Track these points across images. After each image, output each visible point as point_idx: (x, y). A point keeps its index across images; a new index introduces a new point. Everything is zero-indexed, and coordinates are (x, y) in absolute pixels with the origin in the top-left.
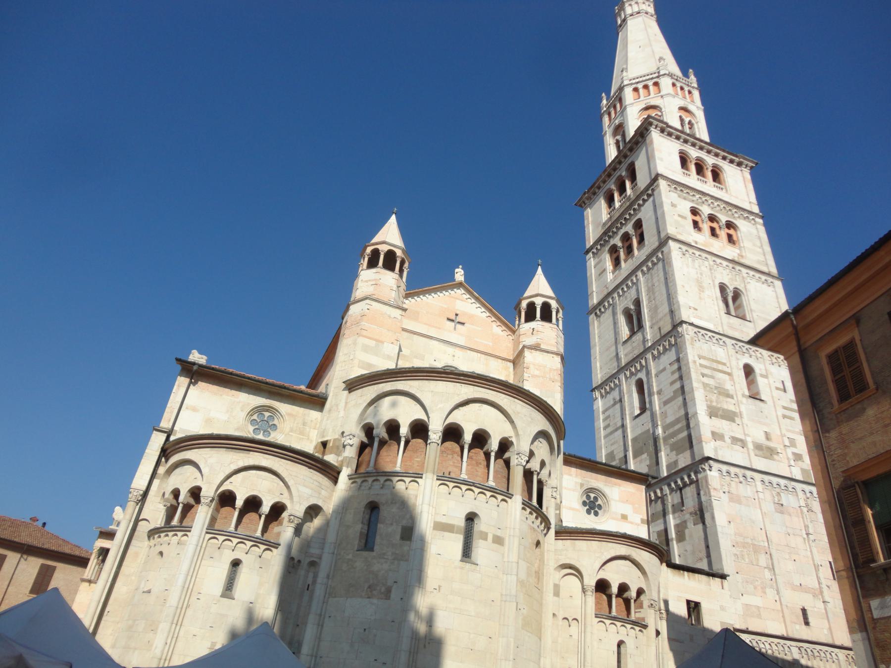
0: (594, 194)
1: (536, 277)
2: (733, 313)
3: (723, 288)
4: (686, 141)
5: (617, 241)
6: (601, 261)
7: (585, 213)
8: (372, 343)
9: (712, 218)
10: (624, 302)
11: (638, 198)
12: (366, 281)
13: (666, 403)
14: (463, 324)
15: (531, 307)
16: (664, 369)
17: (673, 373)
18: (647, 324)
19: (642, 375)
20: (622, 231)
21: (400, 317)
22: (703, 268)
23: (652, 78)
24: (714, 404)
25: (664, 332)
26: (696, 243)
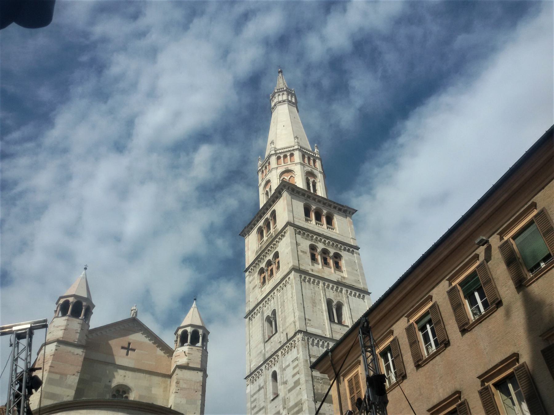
0: (252, 228)
1: (192, 309)
2: (336, 321)
3: (329, 303)
4: (309, 197)
5: (263, 265)
6: (254, 279)
7: (246, 241)
8: (57, 377)
9: (325, 252)
10: (268, 312)
11: (277, 236)
12: (57, 327)
13: (290, 390)
14: (134, 350)
15: (185, 334)
16: (289, 365)
17: (294, 368)
18: (280, 329)
19: (276, 368)
20: (267, 259)
21: (81, 353)
22: (316, 289)
23: (290, 151)
24: (320, 391)
25: (290, 336)
26: (312, 271)
